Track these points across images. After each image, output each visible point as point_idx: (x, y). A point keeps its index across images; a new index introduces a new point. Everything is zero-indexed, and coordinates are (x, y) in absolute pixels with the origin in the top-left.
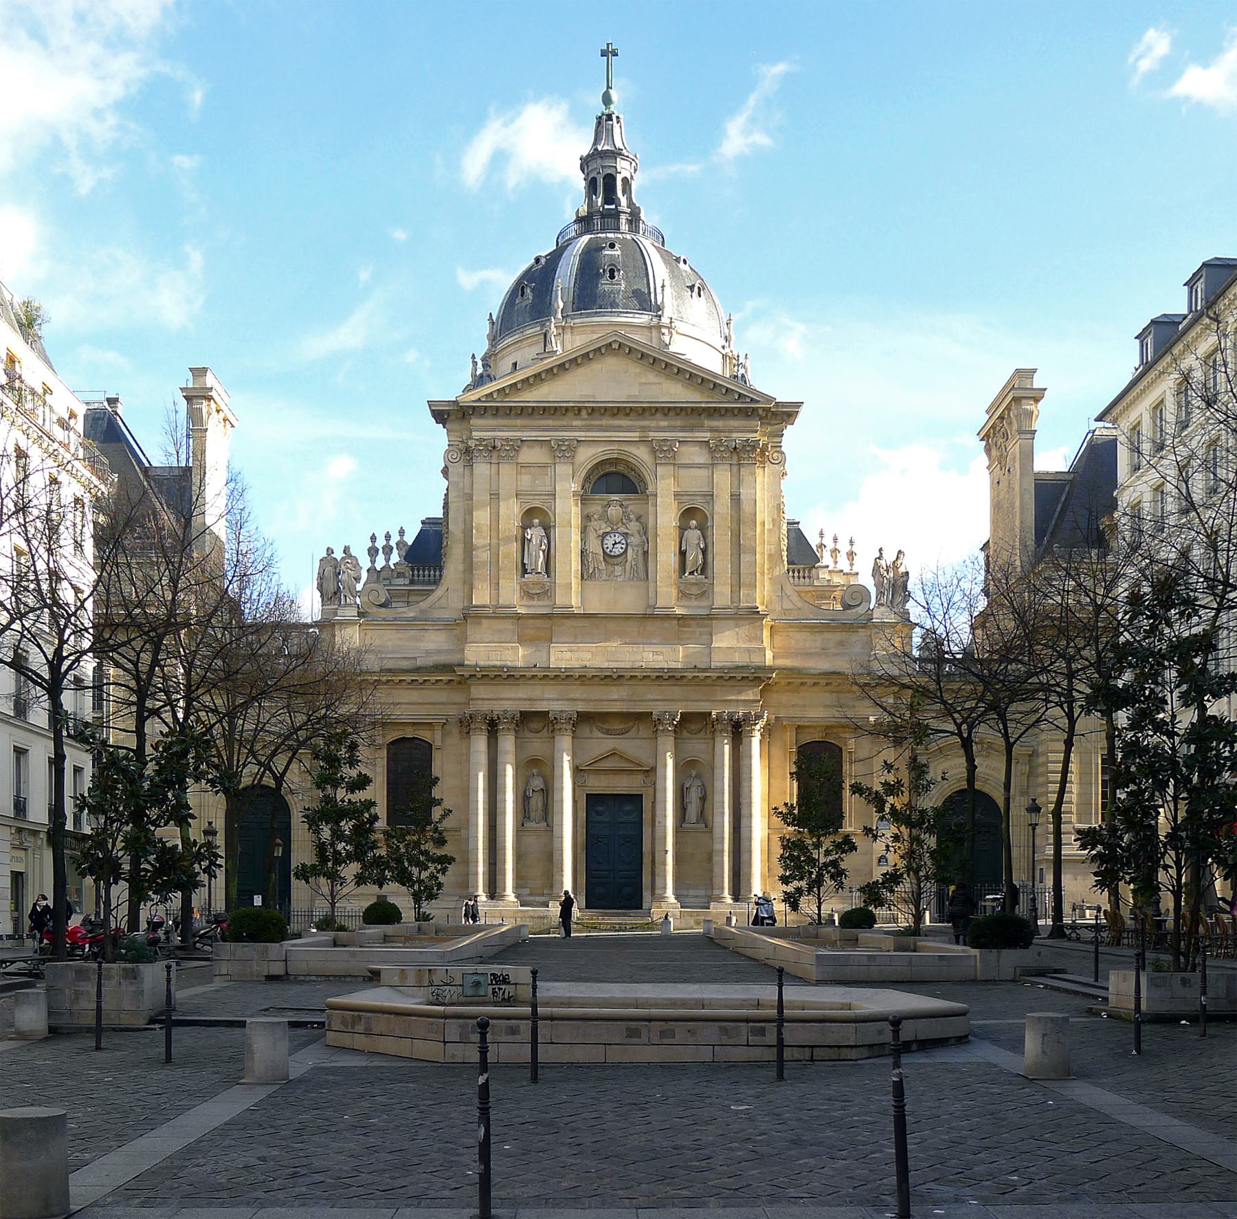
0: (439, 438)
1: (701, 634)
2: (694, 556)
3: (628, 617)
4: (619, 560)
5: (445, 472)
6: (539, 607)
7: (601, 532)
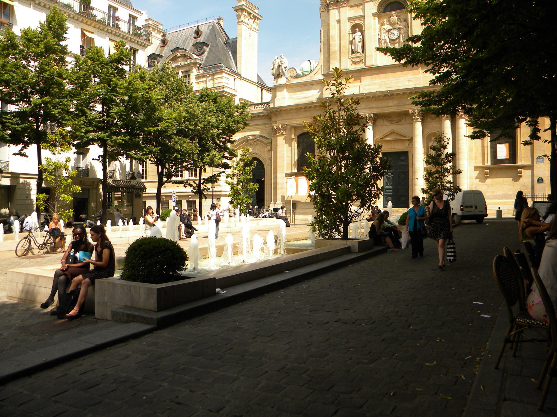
7: (387, 30)
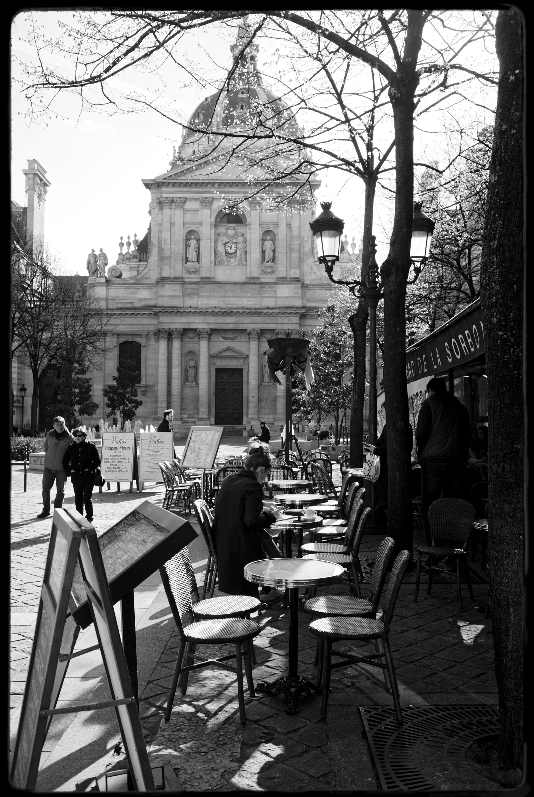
0: (147, 195)
1: (271, 291)
2: (269, 254)
3: (235, 283)
4: (233, 255)
5: (150, 212)
6: (195, 278)
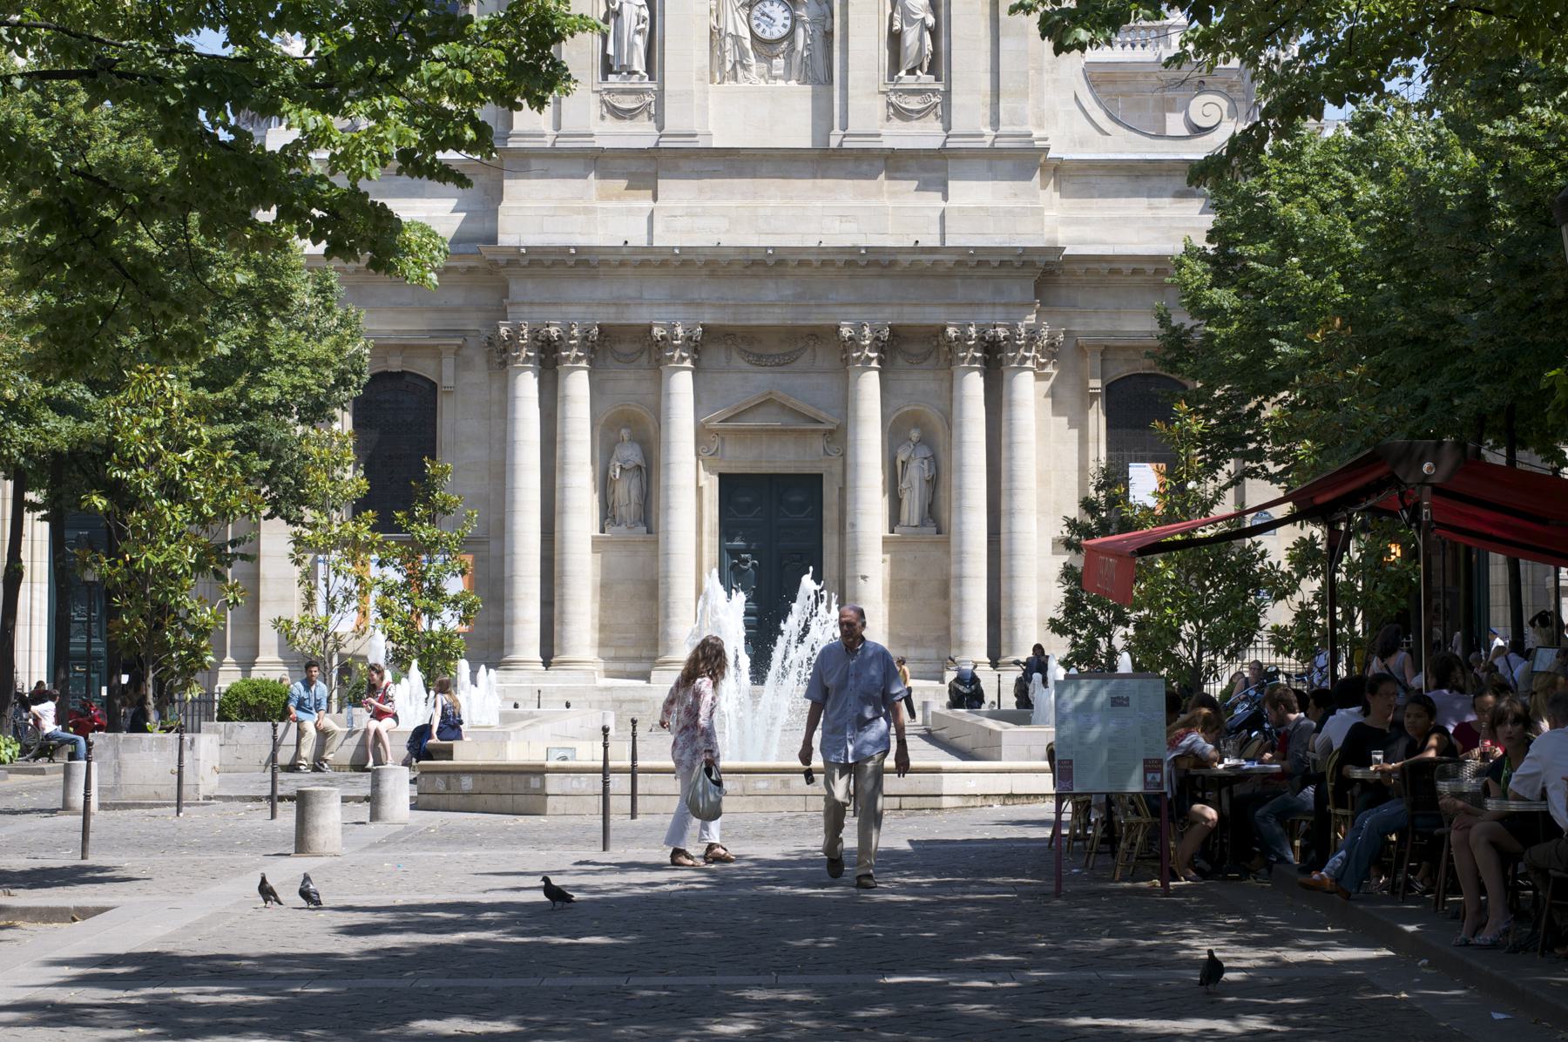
6: (639, 135)
